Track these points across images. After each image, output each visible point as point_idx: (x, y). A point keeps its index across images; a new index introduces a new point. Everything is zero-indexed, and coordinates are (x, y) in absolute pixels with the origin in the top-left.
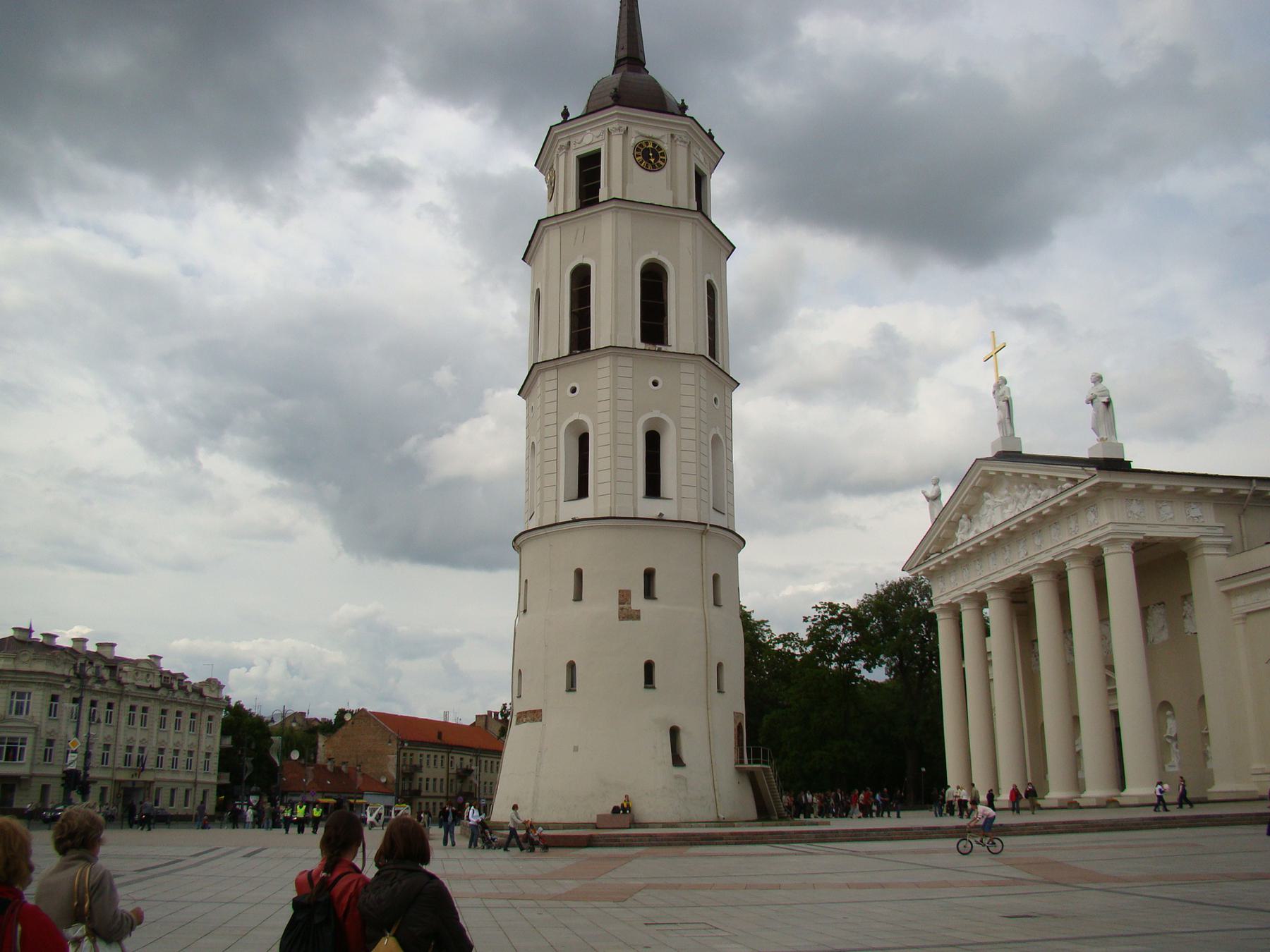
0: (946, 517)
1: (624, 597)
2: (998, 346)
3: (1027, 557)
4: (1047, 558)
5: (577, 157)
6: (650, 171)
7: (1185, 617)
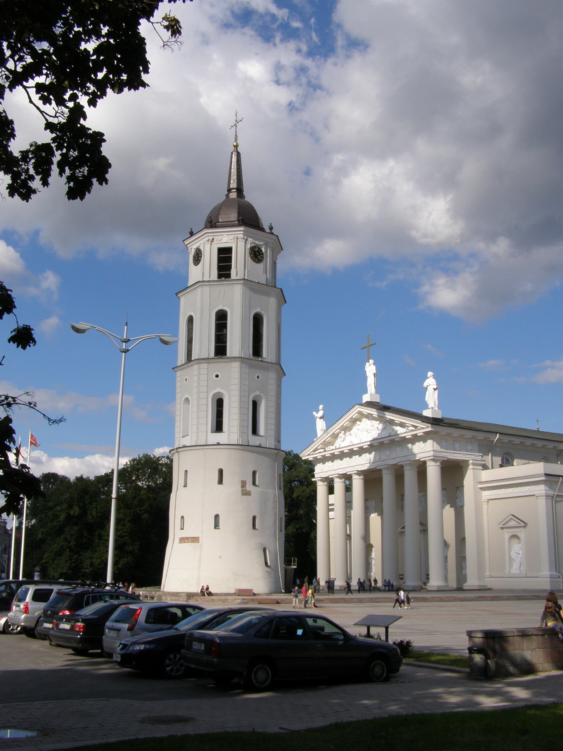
0: (331, 431)
1: (244, 484)
2: (371, 343)
3: (380, 460)
4: (394, 462)
5: (218, 248)
6: (256, 263)
7: (457, 498)
